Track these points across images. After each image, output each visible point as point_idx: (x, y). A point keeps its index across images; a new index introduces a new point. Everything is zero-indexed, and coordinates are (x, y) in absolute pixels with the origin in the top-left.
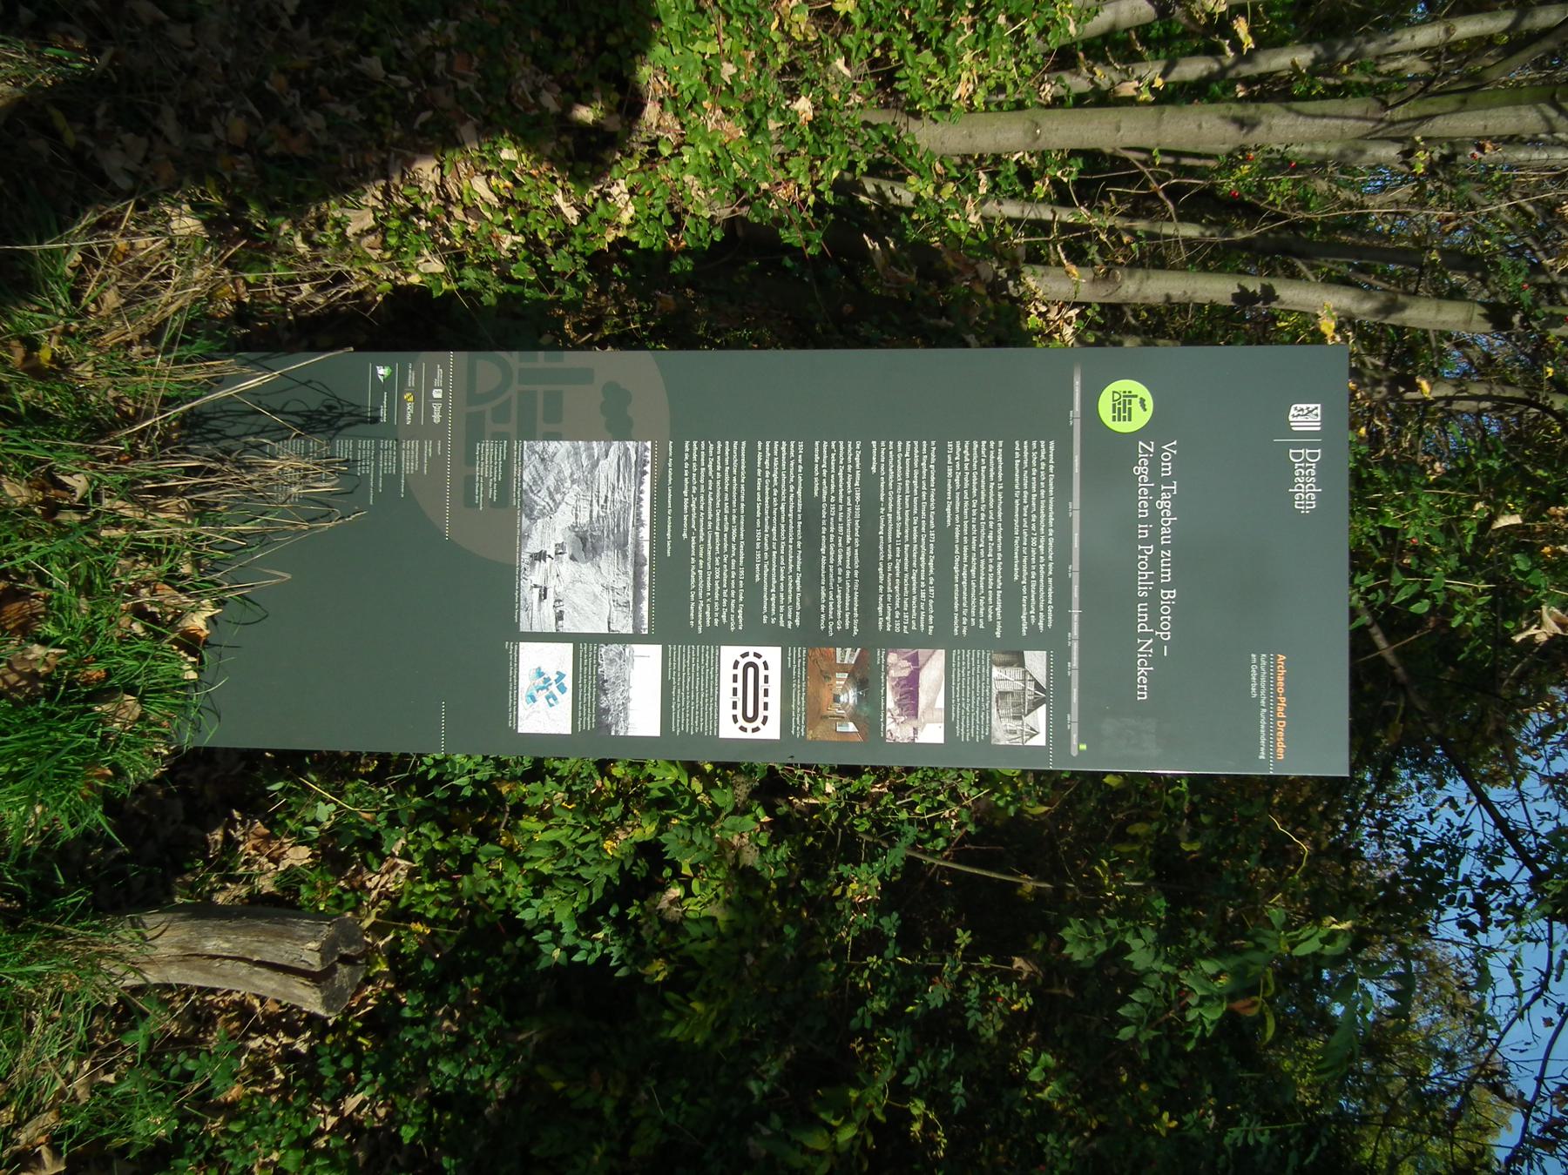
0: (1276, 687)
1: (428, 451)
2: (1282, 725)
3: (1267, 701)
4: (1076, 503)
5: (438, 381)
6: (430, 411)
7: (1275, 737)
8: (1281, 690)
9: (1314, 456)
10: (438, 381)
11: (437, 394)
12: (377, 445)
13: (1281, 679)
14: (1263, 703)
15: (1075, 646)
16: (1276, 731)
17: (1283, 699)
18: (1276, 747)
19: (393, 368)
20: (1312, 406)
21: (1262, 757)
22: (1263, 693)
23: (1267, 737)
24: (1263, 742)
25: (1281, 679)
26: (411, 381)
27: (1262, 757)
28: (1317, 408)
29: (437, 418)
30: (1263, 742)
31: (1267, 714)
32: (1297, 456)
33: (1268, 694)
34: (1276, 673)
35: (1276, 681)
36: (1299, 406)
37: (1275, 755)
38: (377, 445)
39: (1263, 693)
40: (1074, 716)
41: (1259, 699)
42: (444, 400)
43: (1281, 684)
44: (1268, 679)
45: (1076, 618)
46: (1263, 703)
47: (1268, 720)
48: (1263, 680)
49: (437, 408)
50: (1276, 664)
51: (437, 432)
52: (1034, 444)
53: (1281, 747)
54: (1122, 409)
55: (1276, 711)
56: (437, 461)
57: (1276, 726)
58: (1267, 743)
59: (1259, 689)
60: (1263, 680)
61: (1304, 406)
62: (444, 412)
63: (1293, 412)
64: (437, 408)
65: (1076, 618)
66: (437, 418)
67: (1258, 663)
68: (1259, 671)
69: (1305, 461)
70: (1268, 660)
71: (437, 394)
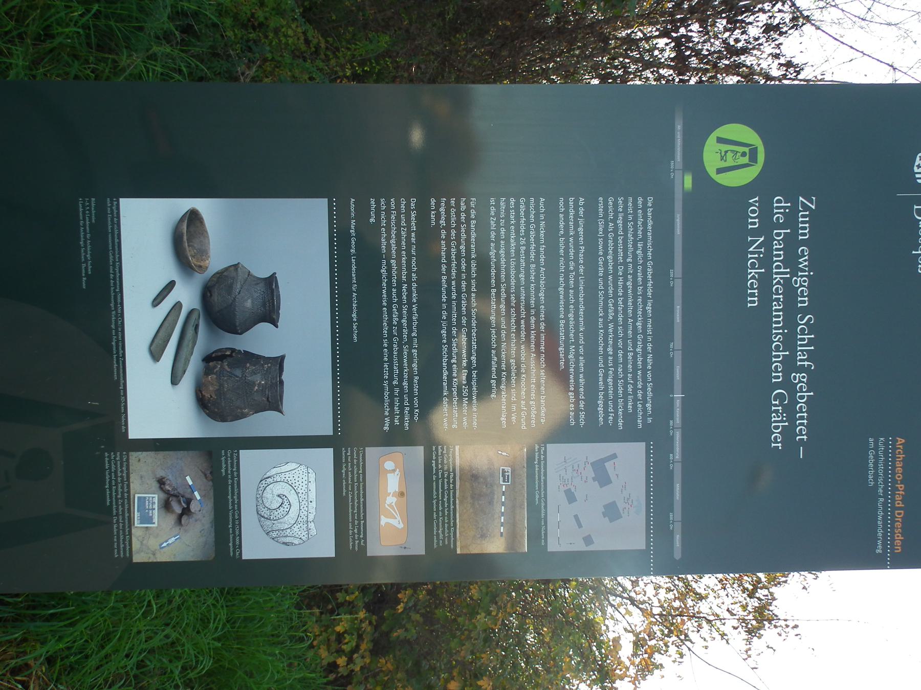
0: (894, 474)
2: (899, 515)
3: (885, 490)
7: (893, 528)
8: (899, 477)
13: (899, 465)
14: (880, 491)
16: (893, 521)
18: (893, 540)
21: (879, 551)
22: (880, 480)
23: (885, 528)
24: (880, 534)
25: (899, 465)
27: (879, 551)
30: (880, 534)
31: (885, 504)
33: (885, 482)
34: (894, 458)
35: (894, 467)
37: (892, 545)
39: (880, 480)
41: (876, 486)
43: (899, 470)
46: (880, 491)
47: (885, 511)
48: (881, 467)
50: (894, 448)
53: (899, 538)
55: (893, 500)
57: (893, 516)
58: (885, 536)
59: (876, 476)
60: (881, 467)
67: (876, 448)
68: (876, 457)
70: (886, 444)
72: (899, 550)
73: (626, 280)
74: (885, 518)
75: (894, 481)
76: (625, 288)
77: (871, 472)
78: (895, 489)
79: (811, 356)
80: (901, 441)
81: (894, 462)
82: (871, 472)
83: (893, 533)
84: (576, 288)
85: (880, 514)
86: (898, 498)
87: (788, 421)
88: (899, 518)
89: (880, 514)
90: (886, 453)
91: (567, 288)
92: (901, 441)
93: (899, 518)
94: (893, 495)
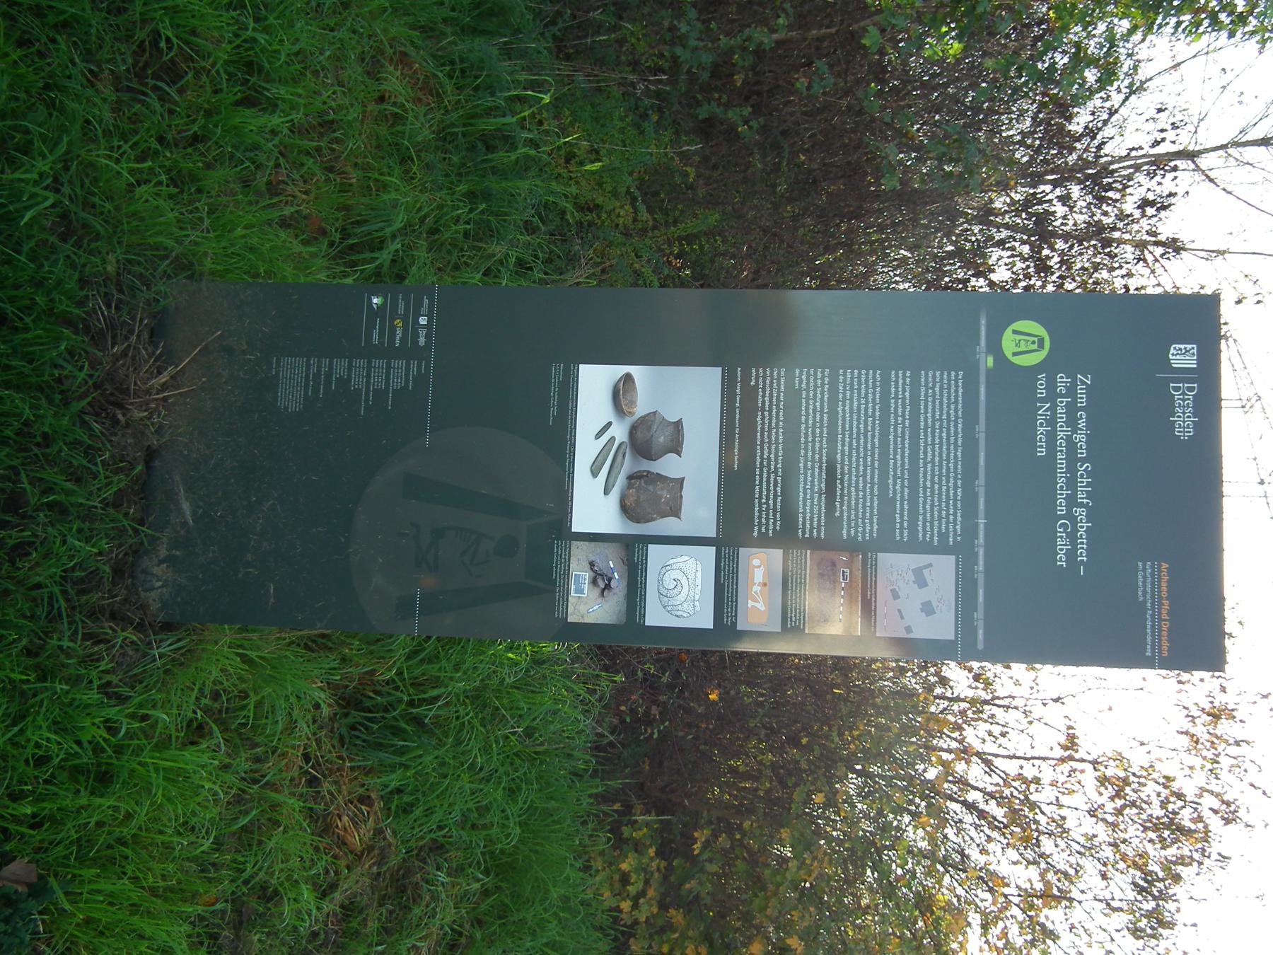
0: (1160, 592)
2: (1166, 626)
3: (1153, 604)
4: (982, 426)
7: (1160, 636)
9: (1191, 389)
10: (424, 310)
11: (423, 321)
12: (369, 363)
13: (1164, 584)
14: (1149, 605)
15: (981, 552)
16: (1160, 630)
17: (1166, 602)
18: (1160, 646)
19: (385, 298)
20: (1189, 347)
21: (1148, 654)
22: (1148, 596)
24: (1149, 639)
25: (1164, 584)
26: (401, 310)
27: (1148, 654)
28: (1192, 347)
29: (422, 341)
30: (1149, 639)
31: (1153, 616)
32: (1177, 389)
33: (1153, 597)
36: (1178, 346)
37: (1160, 649)
38: (369, 363)
39: (1148, 596)
40: (980, 614)
41: (1145, 601)
42: (429, 326)
43: (1164, 589)
44: (1153, 585)
45: (982, 527)
46: (1149, 605)
47: (1153, 621)
49: (422, 333)
50: (1160, 571)
52: (953, 374)
53: (1165, 645)
55: (1160, 614)
56: (421, 379)
57: (1160, 626)
59: (1145, 593)
61: (1182, 346)
63: (1172, 351)
64: (422, 333)
65: (982, 527)
66: (422, 341)
67: (1144, 570)
68: (1145, 577)
69: (1184, 394)
70: (1152, 567)
72: (1165, 654)
73: (941, 432)
74: (1153, 627)
75: (1160, 598)
76: (941, 438)
77: (1141, 589)
78: (1160, 604)
79: (1089, 495)
80: (1165, 566)
81: (1159, 582)
82: (1141, 589)
83: (1160, 640)
84: (903, 437)
85: (1149, 624)
86: (1164, 612)
87: (1072, 542)
88: (1165, 628)
89: (1149, 624)
90: (1152, 574)
91: (896, 437)
92: (1165, 566)
93: (1165, 628)
94: (1160, 609)
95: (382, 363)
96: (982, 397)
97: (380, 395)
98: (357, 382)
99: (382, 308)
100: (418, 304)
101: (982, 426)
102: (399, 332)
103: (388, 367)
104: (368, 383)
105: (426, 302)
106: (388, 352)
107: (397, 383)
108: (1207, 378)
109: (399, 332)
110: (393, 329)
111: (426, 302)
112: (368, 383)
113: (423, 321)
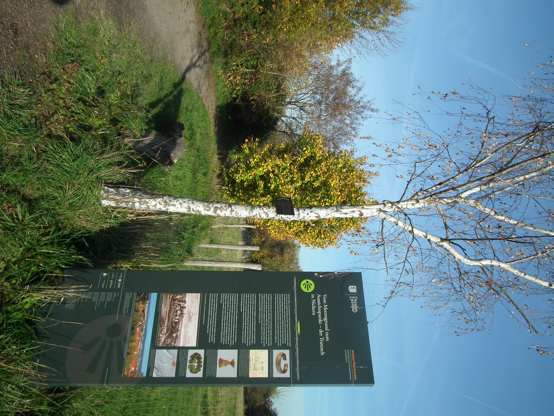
1: (115, 295)
4: (296, 310)
5: (121, 277)
6: (117, 285)
8: (354, 360)
10: (121, 277)
13: (353, 357)
15: (297, 348)
25: (353, 357)
26: (113, 277)
29: (119, 287)
45: (297, 341)
49: (119, 284)
51: (119, 290)
53: (355, 376)
54: (307, 286)
62: (121, 285)
64: (119, 284)
65: (297, 341)
66: (119, 287)
71: (120, 280)
80: (353, 351)
92: (353, 351)
95: (105, 293)
96: (296, 301)
97: (102, 303)
98: (95, 299)
99: (107, 276)
100: (119, 275)
101: (296, 310)
102: (111, 284)
103: (106, 295)
104: (99, 300)
105: (122, 275)
106: (107, 290)
107: (109, 300)
108: (360, 293)
109: (111, 284)
110: (109, 283)
111: (122, 275)
112: (99, 300)
113: (120, 280)
